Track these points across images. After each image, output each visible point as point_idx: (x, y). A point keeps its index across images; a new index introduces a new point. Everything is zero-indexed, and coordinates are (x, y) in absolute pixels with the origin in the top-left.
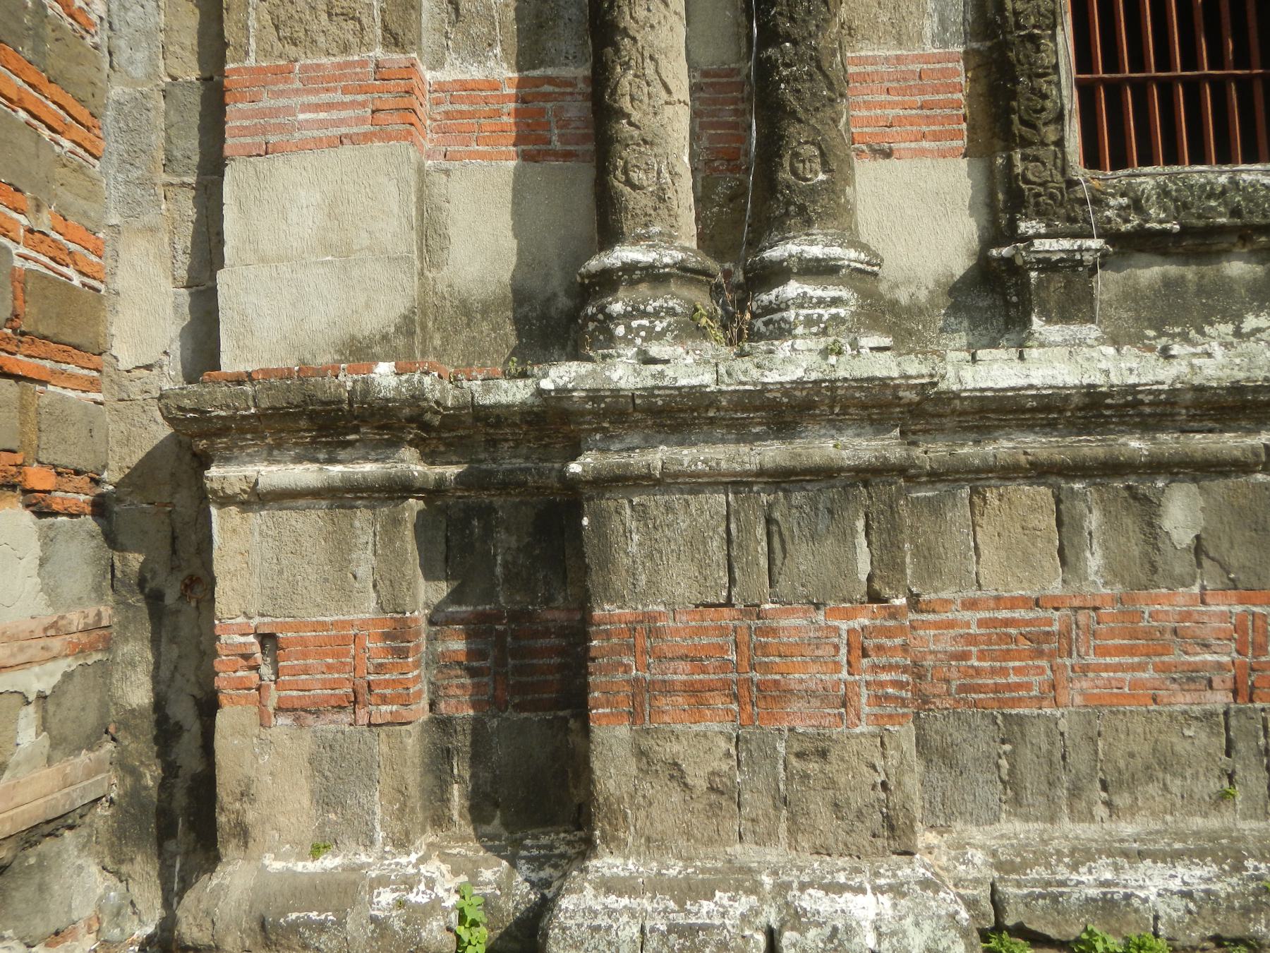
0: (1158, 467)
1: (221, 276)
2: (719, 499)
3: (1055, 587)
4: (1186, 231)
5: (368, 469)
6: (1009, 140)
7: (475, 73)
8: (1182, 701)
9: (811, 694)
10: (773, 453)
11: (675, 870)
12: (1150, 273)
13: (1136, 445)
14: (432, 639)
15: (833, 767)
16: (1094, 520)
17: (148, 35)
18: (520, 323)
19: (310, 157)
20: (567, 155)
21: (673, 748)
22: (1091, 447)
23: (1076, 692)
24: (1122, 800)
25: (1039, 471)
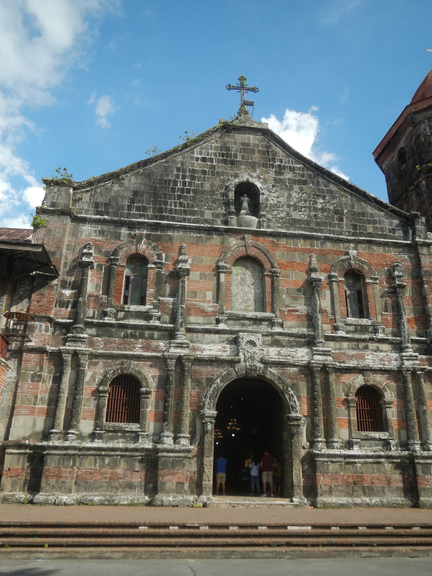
0: (105, 455)
1: (11, 429)
2: (59, 457)
3: (93, 468)
4: (113, 430)
5: (23, 451)
6: (98, 419)
7: (43, 406)
8: (104, 480)
9: (64, 477)
10: (64, 452)
11: (47, 494)
12: (110, 434)
13: (103, 453)
14: (27, 470)
15: (65, 484)
16: (98, 461)
17: (7, 400)
18: (43, 435)
19: (23, 416)
20: (51, 417)
21: (49, 482)
22: (98, 453)
23: (93, 479)
24: (96, 490)
25: (93, 455)
